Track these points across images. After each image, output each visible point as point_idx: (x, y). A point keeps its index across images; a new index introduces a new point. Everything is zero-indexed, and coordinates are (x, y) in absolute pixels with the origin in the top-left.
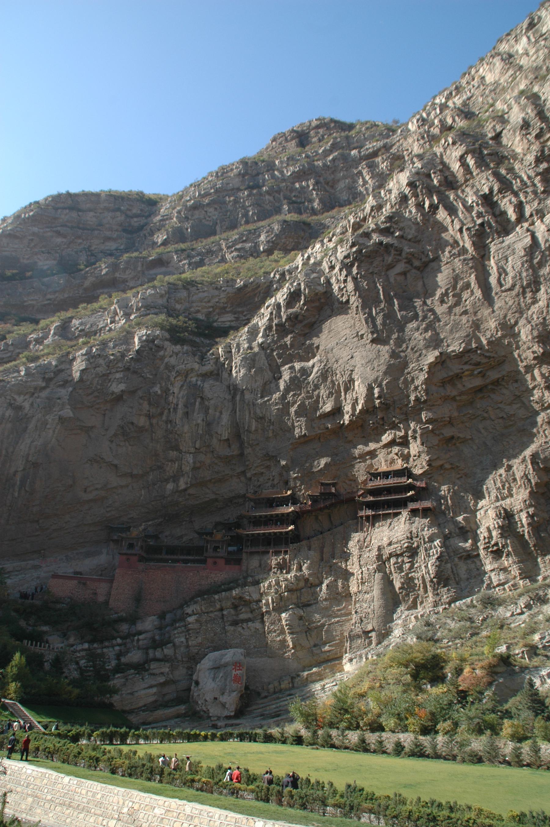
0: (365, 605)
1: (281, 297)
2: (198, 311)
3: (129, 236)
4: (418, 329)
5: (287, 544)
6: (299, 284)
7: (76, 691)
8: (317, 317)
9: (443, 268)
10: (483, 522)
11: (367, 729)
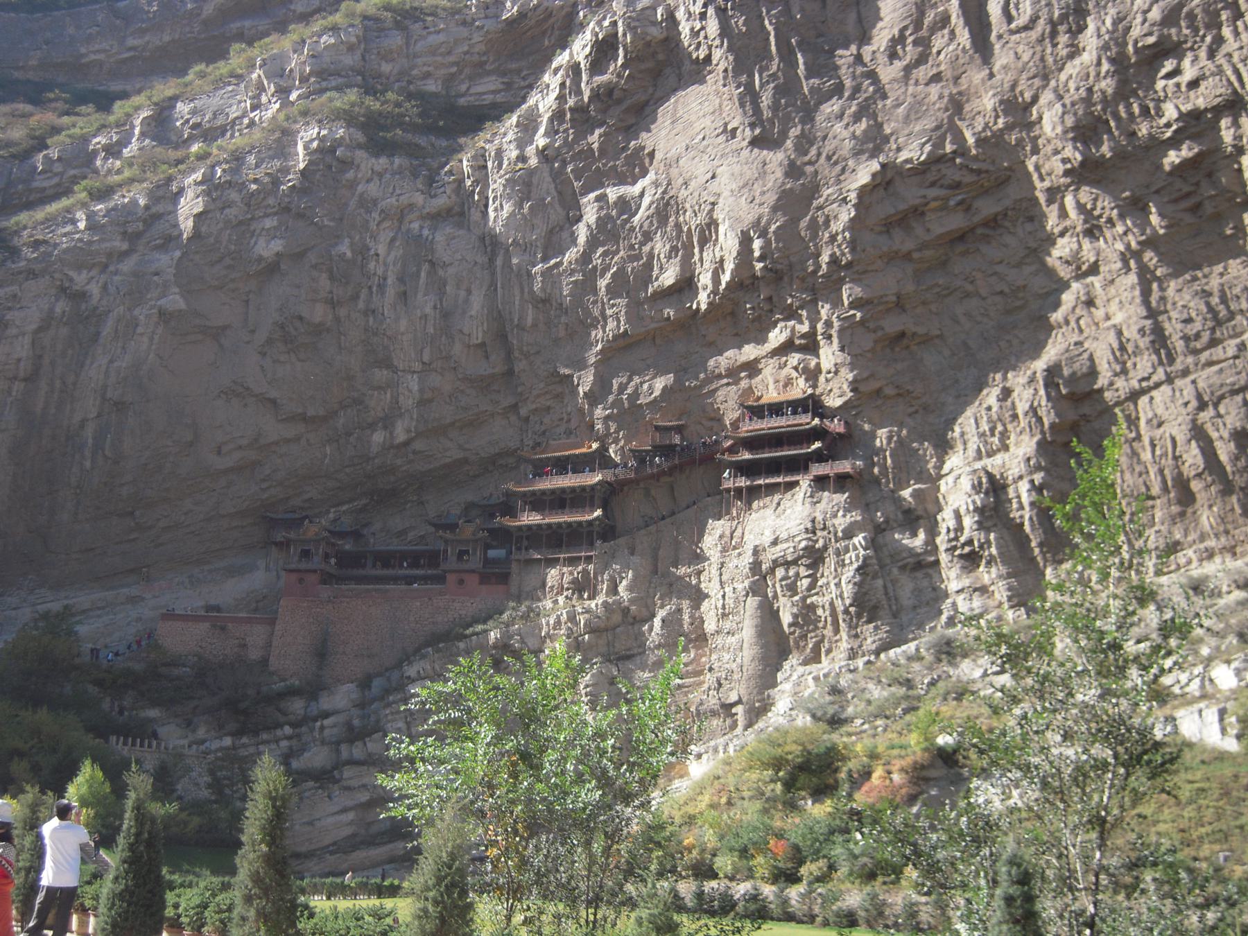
0: (726, 657)
1: (580, 48)
2: (427, 75)
4: (840, 116)
5: (591, 545)
6: (614, 24)
7: (196, 821)
8: (650, 90)
10: (950, 499)
11: (687, 877)
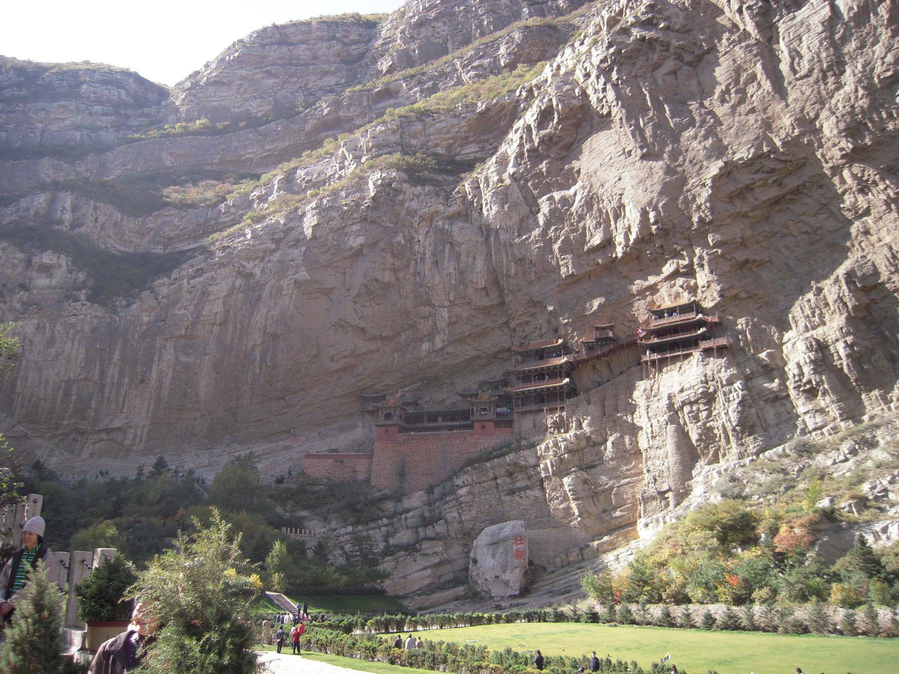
0: (658, 462)
1: (530, 117)
2: (437, 145)
3: (350, 67)
4: (695, 137)
5: (562, 399)
6: (550, 100)
7: (345, 579)
8: (575, 136)
9: (721, 60)
10: (791, 357)
